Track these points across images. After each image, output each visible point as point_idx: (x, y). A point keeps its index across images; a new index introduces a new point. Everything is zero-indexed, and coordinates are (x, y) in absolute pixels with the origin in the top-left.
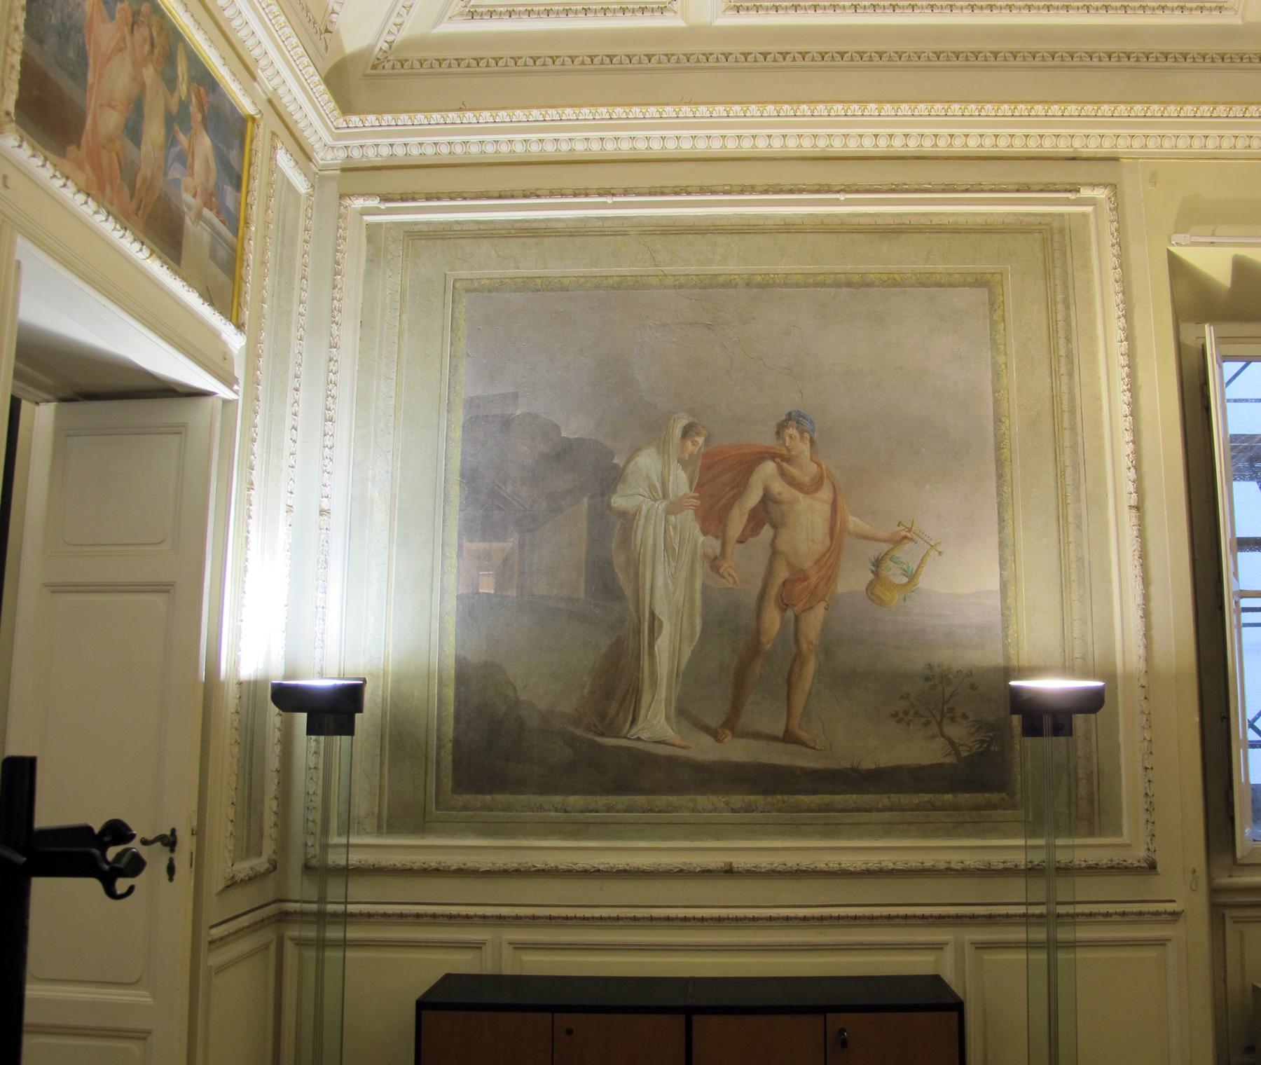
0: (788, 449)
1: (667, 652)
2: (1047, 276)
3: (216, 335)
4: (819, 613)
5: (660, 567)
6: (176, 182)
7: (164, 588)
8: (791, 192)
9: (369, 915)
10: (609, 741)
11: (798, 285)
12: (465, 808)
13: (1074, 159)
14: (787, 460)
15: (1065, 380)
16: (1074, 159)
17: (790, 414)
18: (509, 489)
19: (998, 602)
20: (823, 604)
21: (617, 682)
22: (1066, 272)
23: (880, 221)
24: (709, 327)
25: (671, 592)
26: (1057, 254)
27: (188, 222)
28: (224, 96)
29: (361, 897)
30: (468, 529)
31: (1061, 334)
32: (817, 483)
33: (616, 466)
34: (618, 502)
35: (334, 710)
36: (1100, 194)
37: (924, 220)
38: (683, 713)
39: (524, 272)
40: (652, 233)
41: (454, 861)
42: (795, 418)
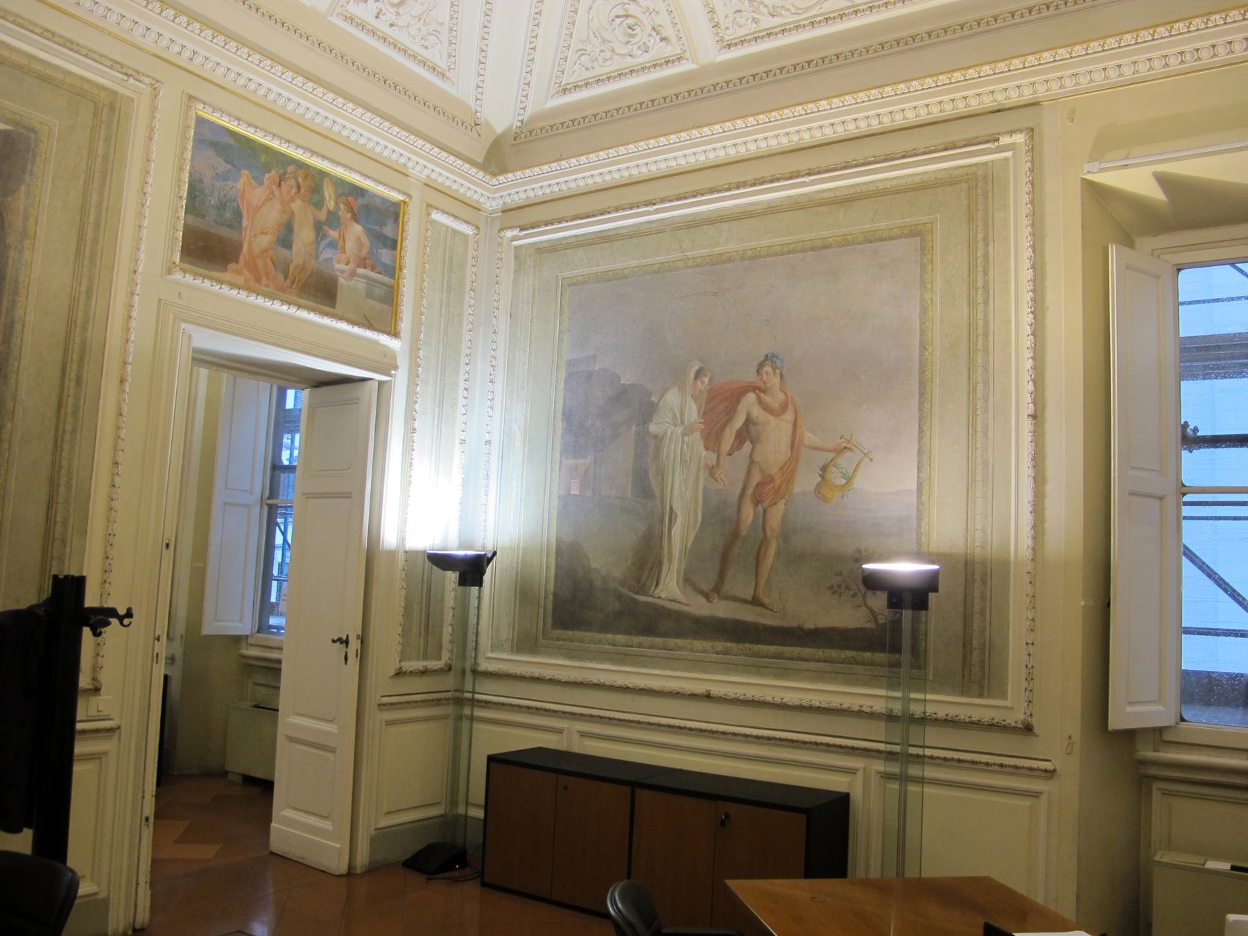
0: (765, 383)
1: (680, 537)
2: (970, 219)
3: (377, 343)
4: (781, 506)
5: (677, 474)
6: (329, 260)
7: (348, 495)
8: (772, 181)
9: (503, 704)
10: (642, 598)
11: (776, 254)
12: (558, 639)
13: (999, 111)
14: (763, 391)
15: (981, 308)
16: (999, 111)
17: (767, 356)
18: (590, 422)
19: (915, 499)
20: (783, 501)
21: (647, 558)
22: (987, 214)
23: (838, 194)
24: (715, 294)
25: (684, 495)
26: (980, 199)
27: (341, 280)
28: (375, 195)
29: (488, 691)
30: (565, 452)
31: (980, 269)
32: (784, 408)
33: (653, 403)
34: (653, 428)
35: (472, 570)
36: (1019, 138)
37: (872, 187)
38: (688, 580)
39: (602, 268)
40: (679, 228)
41: (548, 673)
42: (769, 359)
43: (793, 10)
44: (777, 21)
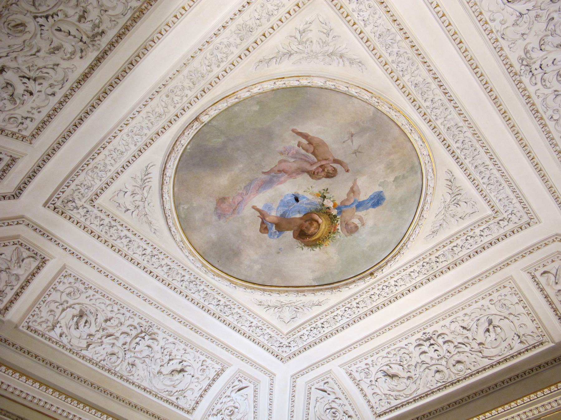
43: (405, 396)
44: (398, 402)
